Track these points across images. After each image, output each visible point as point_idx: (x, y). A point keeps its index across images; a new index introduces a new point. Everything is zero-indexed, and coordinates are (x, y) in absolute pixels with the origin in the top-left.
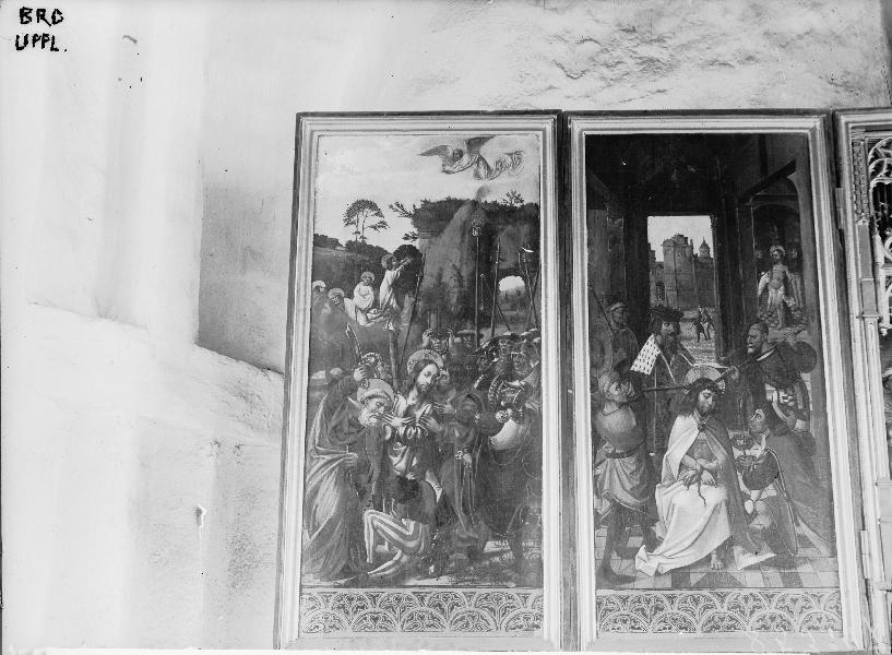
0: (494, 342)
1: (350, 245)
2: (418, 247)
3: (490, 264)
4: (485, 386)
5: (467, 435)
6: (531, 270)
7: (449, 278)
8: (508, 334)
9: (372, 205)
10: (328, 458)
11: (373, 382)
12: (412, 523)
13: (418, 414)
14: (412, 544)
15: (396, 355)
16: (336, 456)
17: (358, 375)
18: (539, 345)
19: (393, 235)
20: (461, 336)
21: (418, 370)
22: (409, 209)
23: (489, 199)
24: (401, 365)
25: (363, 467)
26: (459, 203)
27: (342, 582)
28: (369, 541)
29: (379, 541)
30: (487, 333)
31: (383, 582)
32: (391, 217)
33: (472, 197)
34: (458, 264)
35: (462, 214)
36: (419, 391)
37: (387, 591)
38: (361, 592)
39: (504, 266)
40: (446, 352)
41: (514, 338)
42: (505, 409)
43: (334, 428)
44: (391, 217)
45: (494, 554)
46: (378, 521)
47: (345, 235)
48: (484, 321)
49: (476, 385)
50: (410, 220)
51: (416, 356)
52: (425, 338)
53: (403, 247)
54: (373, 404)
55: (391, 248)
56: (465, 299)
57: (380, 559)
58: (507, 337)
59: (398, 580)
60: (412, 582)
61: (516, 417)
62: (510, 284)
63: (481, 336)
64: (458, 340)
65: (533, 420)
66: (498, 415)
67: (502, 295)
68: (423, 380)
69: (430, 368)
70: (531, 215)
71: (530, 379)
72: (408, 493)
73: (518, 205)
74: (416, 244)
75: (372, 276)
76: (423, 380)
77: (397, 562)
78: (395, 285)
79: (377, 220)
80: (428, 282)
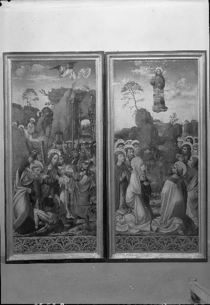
0: (79, 145)
1: (26, 108)
2: (50, 108)
3: (77, 114)
4: (76, 163)
5: (70, 181)
6: (92, 116)
7: (62, 121)
8: (84, 142)
9: (34, 92)
10: (20, 190)
11: (36, 161)
12: (51, 213)
13: (52, 173)
14: (51, 221)
15: (44, 151)
16: (22, 190)
17: (30, 159)
18: (95, 146)
19: (42, 102)
20: (67, 144)
21: (52, 156)
22: (47, 93)
23: (77, 88)
24: (46, 155)
25: (33, 193)
26: (66, 90)
27: (28, 235)
28: (36, 219)
29: (40, 220)
30: (76, 142)
31: (40, 235)
32: (40, 96)
33: (70, 87)
34: (65, 115)
35: (66, 94)
36: (52, 165)
37: (43, 238)
38: (35, 238)
39: (83, 115)
40: (61, 150)
41: (87, 144)
42: (83, 171)
43: (22, 179)
44: (40, 96)
45: (80, 224)
46: (38, 212)
47: (24, 104)
48: (76, 138)
49: (72, 162)
50: (47, 97)
51: (52, 151)
52: (54, 144)
53: (45, 108)
54: (36, 170)
55: (41, 109)
56: (68, 129)
57: (40, 227)
58: (84, 144)
59: (46, 233)
60: (52, 234)
61: (87, 174)
62: (85, 122)
63: (74, 143)
64: (66, 145)
65: (92, 175)
66: (81, 173)
67: (82, 127)
68: (54, 161)
69: (56, 156)
70: (93, 94)
71: (92, 160)
72: (48, 204)
73: (88, 90)
74: (50, 107)
75: (34, 120)
76: (54, 161)
77: (46, 227)
78: (43, 123)
79: (33, 97)
80: (55, 123)
